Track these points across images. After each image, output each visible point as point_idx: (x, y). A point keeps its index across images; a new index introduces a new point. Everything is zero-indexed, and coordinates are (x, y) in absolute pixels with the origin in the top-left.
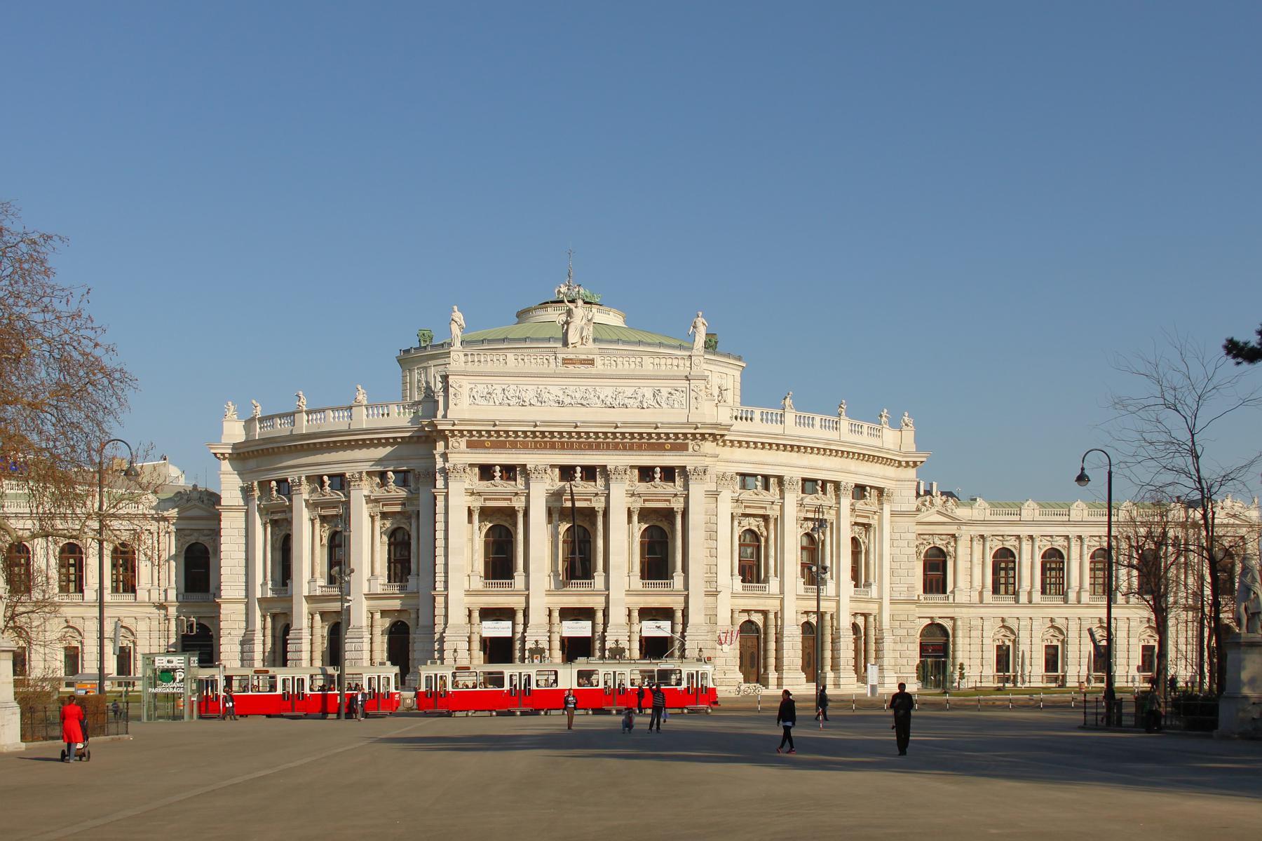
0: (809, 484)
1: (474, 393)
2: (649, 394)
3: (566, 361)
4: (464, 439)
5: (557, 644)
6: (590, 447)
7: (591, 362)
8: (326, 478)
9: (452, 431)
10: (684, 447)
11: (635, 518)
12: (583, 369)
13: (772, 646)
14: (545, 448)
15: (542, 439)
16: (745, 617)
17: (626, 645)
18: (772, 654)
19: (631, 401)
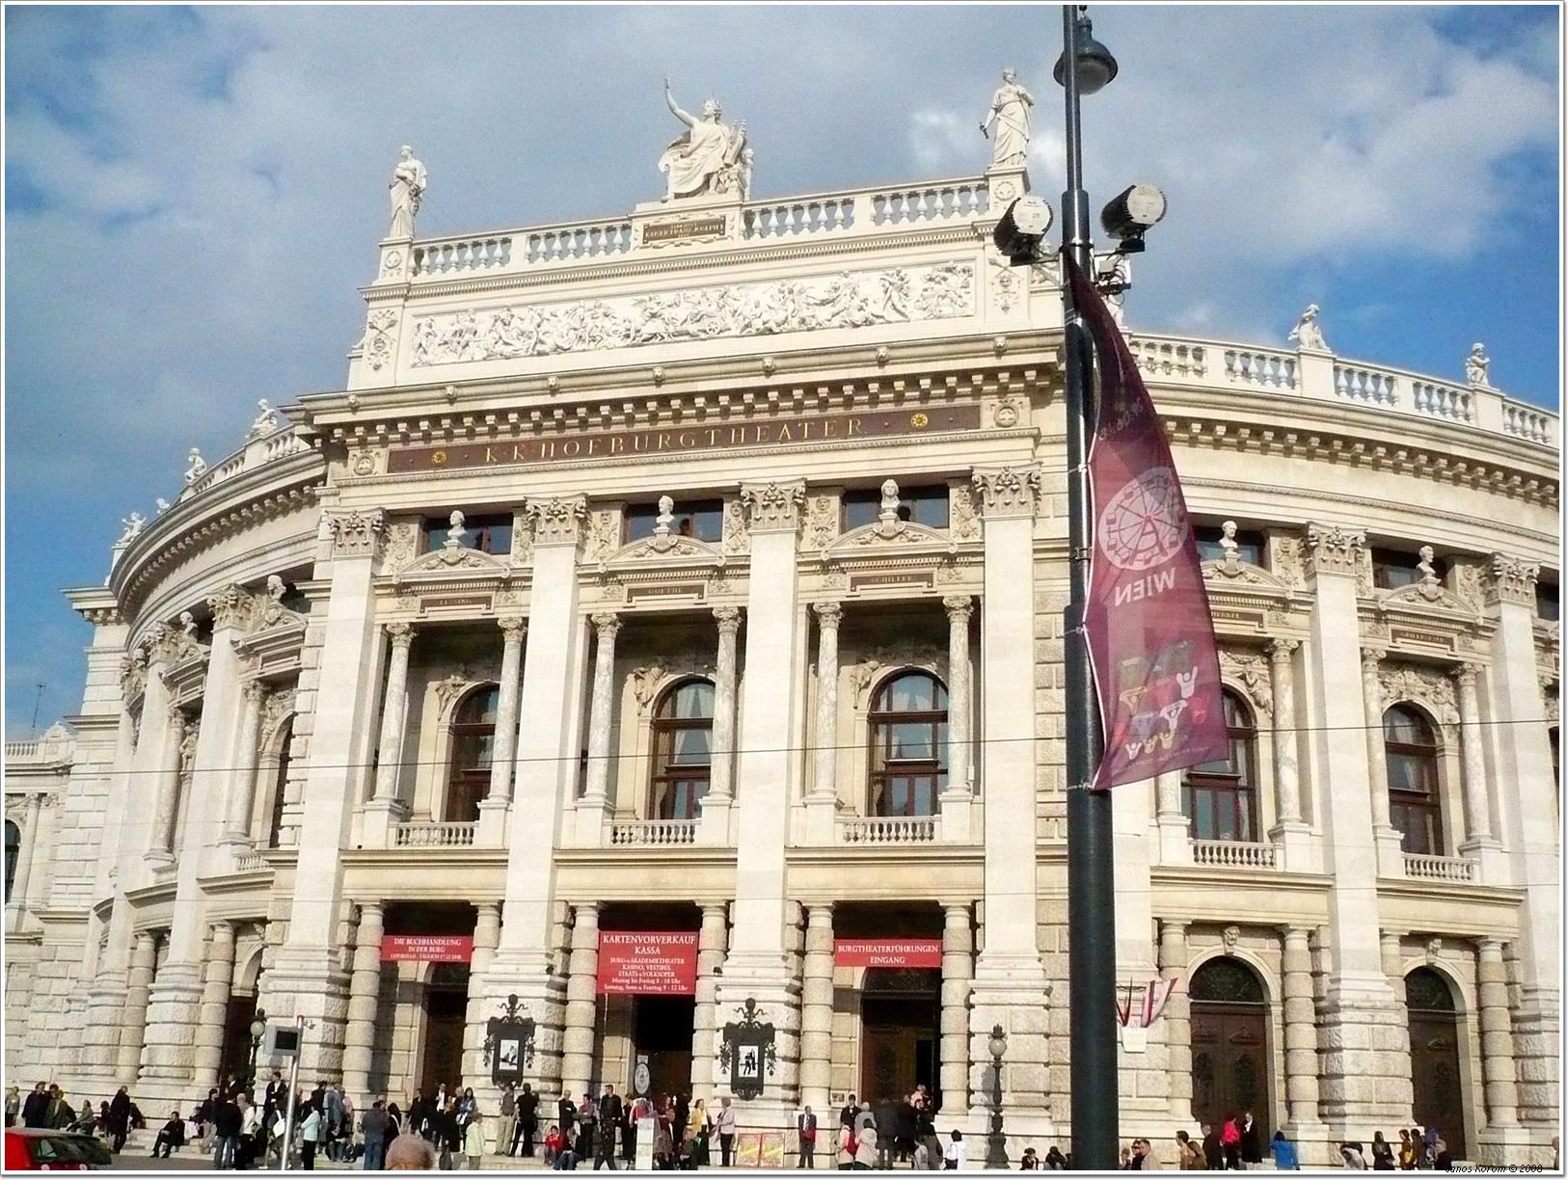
0: (1393, 557)
1: (421, 338)
2: (871, 287)
3: (652, 233)
4: (384, 452)
5: (581, 1011)
6: (701, 438)
7: (717, 227)
8: (185, 617)
9: (349, 428)
10: (968, 418)
11: (829, 637)
12: (697, 246)
13: (1305, 1036)
14: (583, 453)
15: (569, 424)
16: (1211, 947)
17: (780, 1017)
18: (1306, 1062)
19: (824, 313)
